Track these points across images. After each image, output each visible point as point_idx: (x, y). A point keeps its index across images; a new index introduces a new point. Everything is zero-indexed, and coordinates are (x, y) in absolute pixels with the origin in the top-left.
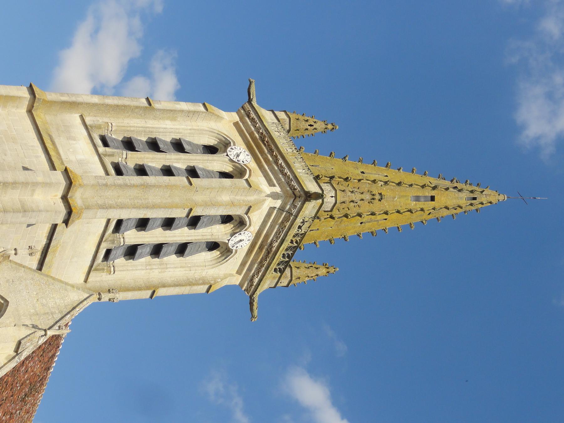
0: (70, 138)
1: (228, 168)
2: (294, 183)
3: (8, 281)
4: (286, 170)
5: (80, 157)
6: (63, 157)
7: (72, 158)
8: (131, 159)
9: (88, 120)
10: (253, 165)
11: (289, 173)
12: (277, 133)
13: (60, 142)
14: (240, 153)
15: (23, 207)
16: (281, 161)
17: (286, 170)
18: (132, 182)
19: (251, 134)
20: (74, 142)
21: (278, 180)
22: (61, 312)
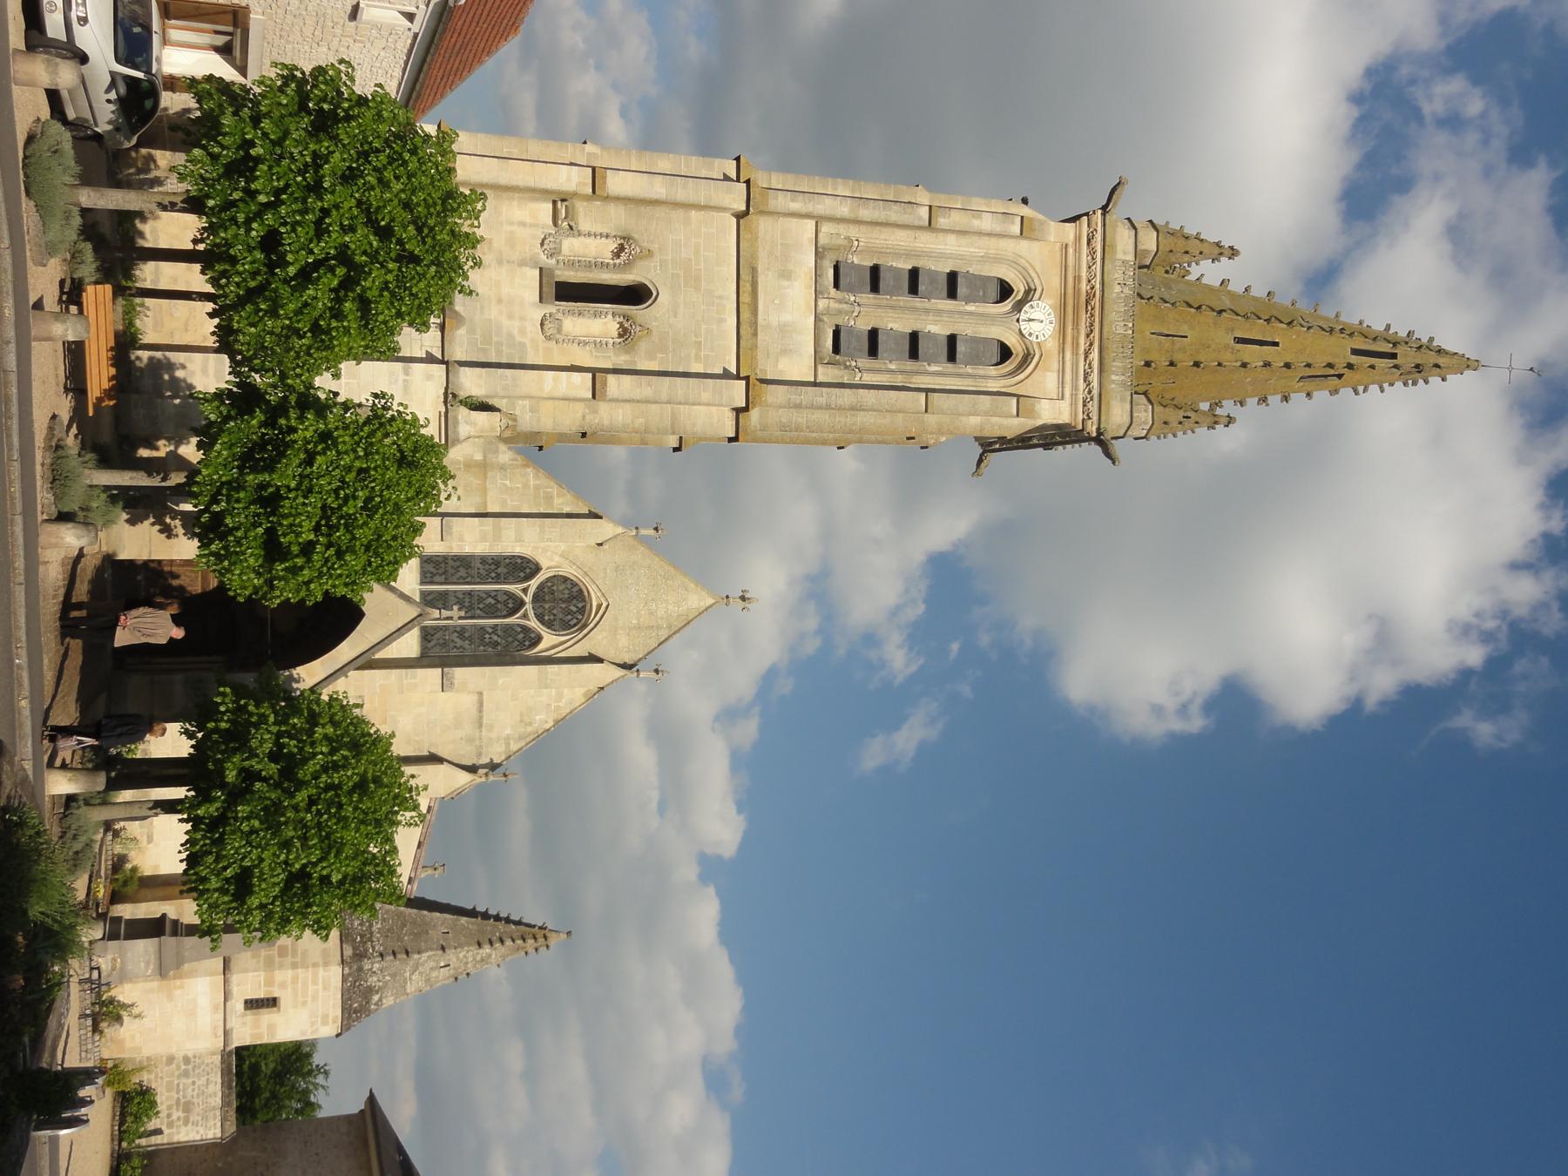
0: (786, 275)
1: (1012, 341)
2: (1093, 407)
3: (617, 569)
4: (1094, 377)
5: (786, 317)
6: (760, 317)
7: (774, 319)
8: (866, 312)
9: (823, 240)
10: (1052, 345)
11: (1095, 384)
12: (1118, 289)
13: (766, 281)
14: (1040, 322)
15: (673, 424)
16: (1095, 355)
17: (1094, 377)
18: (840, 402)
19: (1077, 279)
20: (786, 283)
21: (1075, 387)
22: (670, 627)
